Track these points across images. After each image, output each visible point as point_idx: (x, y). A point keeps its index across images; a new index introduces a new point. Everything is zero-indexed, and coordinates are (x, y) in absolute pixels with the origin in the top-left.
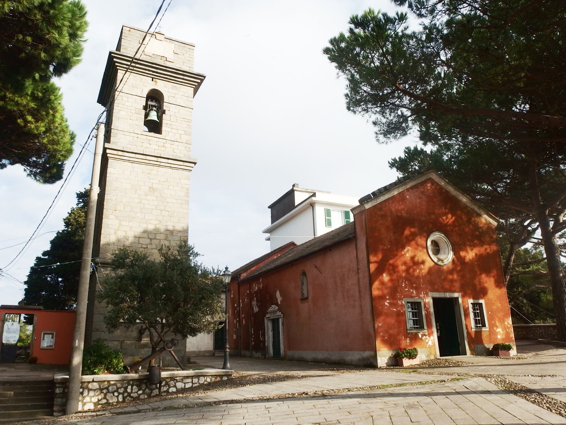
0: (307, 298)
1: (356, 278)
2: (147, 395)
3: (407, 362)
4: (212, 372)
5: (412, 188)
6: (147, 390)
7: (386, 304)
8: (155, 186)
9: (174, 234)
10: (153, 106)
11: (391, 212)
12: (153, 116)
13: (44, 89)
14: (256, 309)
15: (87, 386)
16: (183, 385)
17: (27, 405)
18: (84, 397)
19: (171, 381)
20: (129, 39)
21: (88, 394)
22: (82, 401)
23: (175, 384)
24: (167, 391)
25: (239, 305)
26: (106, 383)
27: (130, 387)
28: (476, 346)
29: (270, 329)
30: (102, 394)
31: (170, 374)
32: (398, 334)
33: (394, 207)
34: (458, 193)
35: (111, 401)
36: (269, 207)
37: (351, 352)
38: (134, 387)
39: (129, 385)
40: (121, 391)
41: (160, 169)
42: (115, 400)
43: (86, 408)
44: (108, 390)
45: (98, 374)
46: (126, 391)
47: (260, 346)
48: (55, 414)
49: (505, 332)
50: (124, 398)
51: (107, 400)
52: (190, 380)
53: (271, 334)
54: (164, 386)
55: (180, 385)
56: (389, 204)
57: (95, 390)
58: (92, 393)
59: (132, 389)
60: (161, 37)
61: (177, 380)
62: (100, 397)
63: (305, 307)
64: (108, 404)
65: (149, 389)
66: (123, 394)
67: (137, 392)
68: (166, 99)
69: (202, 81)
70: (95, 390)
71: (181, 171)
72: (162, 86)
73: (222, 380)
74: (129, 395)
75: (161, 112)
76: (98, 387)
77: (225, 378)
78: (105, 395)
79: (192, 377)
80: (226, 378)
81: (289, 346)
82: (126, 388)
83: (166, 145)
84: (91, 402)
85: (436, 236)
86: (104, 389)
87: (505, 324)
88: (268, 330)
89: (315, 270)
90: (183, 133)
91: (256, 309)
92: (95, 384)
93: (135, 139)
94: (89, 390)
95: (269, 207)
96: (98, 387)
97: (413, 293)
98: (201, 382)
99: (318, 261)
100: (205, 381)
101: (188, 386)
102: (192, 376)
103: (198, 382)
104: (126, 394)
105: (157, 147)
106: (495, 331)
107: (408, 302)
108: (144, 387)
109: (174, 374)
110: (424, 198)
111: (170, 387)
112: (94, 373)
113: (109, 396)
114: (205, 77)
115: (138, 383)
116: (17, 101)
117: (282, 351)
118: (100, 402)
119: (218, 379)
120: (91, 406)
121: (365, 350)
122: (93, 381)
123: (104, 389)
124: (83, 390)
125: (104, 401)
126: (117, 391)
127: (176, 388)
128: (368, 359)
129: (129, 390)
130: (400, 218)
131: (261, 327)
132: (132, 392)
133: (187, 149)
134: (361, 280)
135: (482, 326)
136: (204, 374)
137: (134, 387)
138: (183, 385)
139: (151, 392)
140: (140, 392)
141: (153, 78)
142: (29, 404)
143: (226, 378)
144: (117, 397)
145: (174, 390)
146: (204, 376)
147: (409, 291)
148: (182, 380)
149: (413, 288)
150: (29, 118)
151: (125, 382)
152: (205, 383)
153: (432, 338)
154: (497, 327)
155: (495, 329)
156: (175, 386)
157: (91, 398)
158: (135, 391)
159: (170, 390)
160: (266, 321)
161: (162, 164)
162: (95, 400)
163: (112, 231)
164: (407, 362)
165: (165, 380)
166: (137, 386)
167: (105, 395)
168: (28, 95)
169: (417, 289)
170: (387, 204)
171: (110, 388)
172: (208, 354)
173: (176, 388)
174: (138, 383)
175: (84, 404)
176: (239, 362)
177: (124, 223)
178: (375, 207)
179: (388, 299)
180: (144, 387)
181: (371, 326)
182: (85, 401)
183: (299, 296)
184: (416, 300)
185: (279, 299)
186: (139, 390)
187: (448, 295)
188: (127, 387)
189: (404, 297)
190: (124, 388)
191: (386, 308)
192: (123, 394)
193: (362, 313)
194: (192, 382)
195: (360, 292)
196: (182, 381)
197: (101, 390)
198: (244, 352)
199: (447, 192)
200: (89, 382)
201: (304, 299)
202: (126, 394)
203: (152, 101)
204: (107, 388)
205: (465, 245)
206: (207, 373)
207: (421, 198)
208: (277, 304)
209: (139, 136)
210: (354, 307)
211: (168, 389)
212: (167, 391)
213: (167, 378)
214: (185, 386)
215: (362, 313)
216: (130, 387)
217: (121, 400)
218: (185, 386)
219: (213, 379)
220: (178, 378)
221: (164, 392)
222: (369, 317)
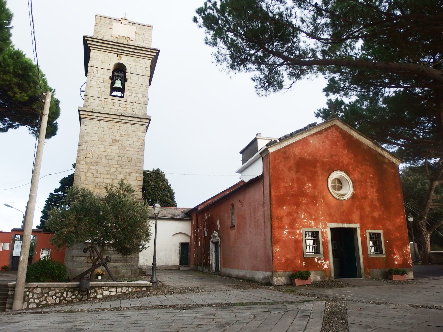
0: (234, 226)
1: (263, 210)
2: (79, 299)
3: (298, 282)
5: (316, 134)
6: (79, 296)
7: (285, 232)
8: (117, 138)
9: (131, 175)
10: (118, 76)
11: (295, 155)
12: (118, 84)
14: (206, 234)
16: (109, 293)
20: (100, 25)
23: (102, 292)
24: (95, 298)
25: (197, 231)
27: (65, 293)
28: (372, 270)
29: (214, 251)
32: (295, 259)
34: (362, 137)
36: (240, 153)
37: (258, 272)
38: (69, 293)
40: (59, 295)
41: (122, 125)
44: (48, 294)
46: (62, 295)
47: (207, 264)
49: (402, 258)
50: (60, 301)
51: (47, 302)
52: (114, 289)
53: (214, 254)
54: (93, 293)
55: (106, 293)
56: (293, 148)
59: (67, 294)
60: (126, 22)
61: (104, 289)
63: (233, 233)
66: (60, 297)
67: (71, 297)
68: (128, 70)
69: (158, 54)
71: (138, 126)
72: (125, 60)
74: (64, 299)
75: (124, 81)
78: (46, 297)
81: (224, 265)
82: (62, 293)
83: (127, 106)
84: (34, 302)
85: (336, 174)
87: (403, 252)
88: (212, 251)
89: (239, 203)
90: (141, 96)
91: (206, 234)
92: (39, 289)
93: (103, 102)
95: (240, 153)
97: (311, 223)
98: (123, 291)
99: (241, 197)
100: (127, 290)
101: (112, 294)
102: (117, 287)
104: (62, 298)
105: (119, 108)
106: (392, 257)
107: (306, 232)
108: (77, 293)
110: (327, 142)
111: (97, 294)
114: (159, 51)
117: (219, 269)
118: (42, 303)
121: (266, 271)
122: (37, 287)
124: (29, 294)
126: (55, 295)
127: (103, 295)
128: (265, 278)
129: (65, 295)
130: (302, 160)
131: (208, 249)
132: (66, 297)
133: (144, 108)
134: (265, 212)
135: (379, 253)
138: (109, 293)
139: (82, 297)
140: (74, 297)
141: (118, 54)
144: (55, 299)
145: (101, 296)
147: (308, 222)
149: (311, 219)
150: (17, 90)
151: (62, 288)
152: (127, 292)
153: (328, 262)
154: (395, 254)
155: (392, 255)
156: (102, 294)
157: (34, 300)
158: (69, 296)
161: (132, 122)
163: (83, 173)
164: (298, 282)
166: (71, 292)
168: (11, 73)
169: (315, 220)
170: (291, 148)
171: (50, 293)
172: (175, 268)
173: (103, 295)
174: (72, 290)
176: (184, 276)
177: (92, 167)
178: (278, 151)
179: (287, 229)
180: (77, 293)
181: (270, 251)
183: (230, 224)
184: (315, 229)
185: (219, 226)
187: (346, 226)
189: (303, 227)
191: (284, 236)
193: (265, 240)
194: (116, 291)
195: (265, 222)
198: (200, 268)
199: (351, 137)
200: (34, 288)
201: (233, 227)
202: (62, 298)
203: (118, 72)
207: (325, 142)
208: (217, 231)
209: (106, 100)
210: (261, 235)
211: (96, 296)
212: (95, 298)
215: (265, 240)
216: (65, 293)
220: (105, 288)
221: (93, 297)
222: (269, 242)
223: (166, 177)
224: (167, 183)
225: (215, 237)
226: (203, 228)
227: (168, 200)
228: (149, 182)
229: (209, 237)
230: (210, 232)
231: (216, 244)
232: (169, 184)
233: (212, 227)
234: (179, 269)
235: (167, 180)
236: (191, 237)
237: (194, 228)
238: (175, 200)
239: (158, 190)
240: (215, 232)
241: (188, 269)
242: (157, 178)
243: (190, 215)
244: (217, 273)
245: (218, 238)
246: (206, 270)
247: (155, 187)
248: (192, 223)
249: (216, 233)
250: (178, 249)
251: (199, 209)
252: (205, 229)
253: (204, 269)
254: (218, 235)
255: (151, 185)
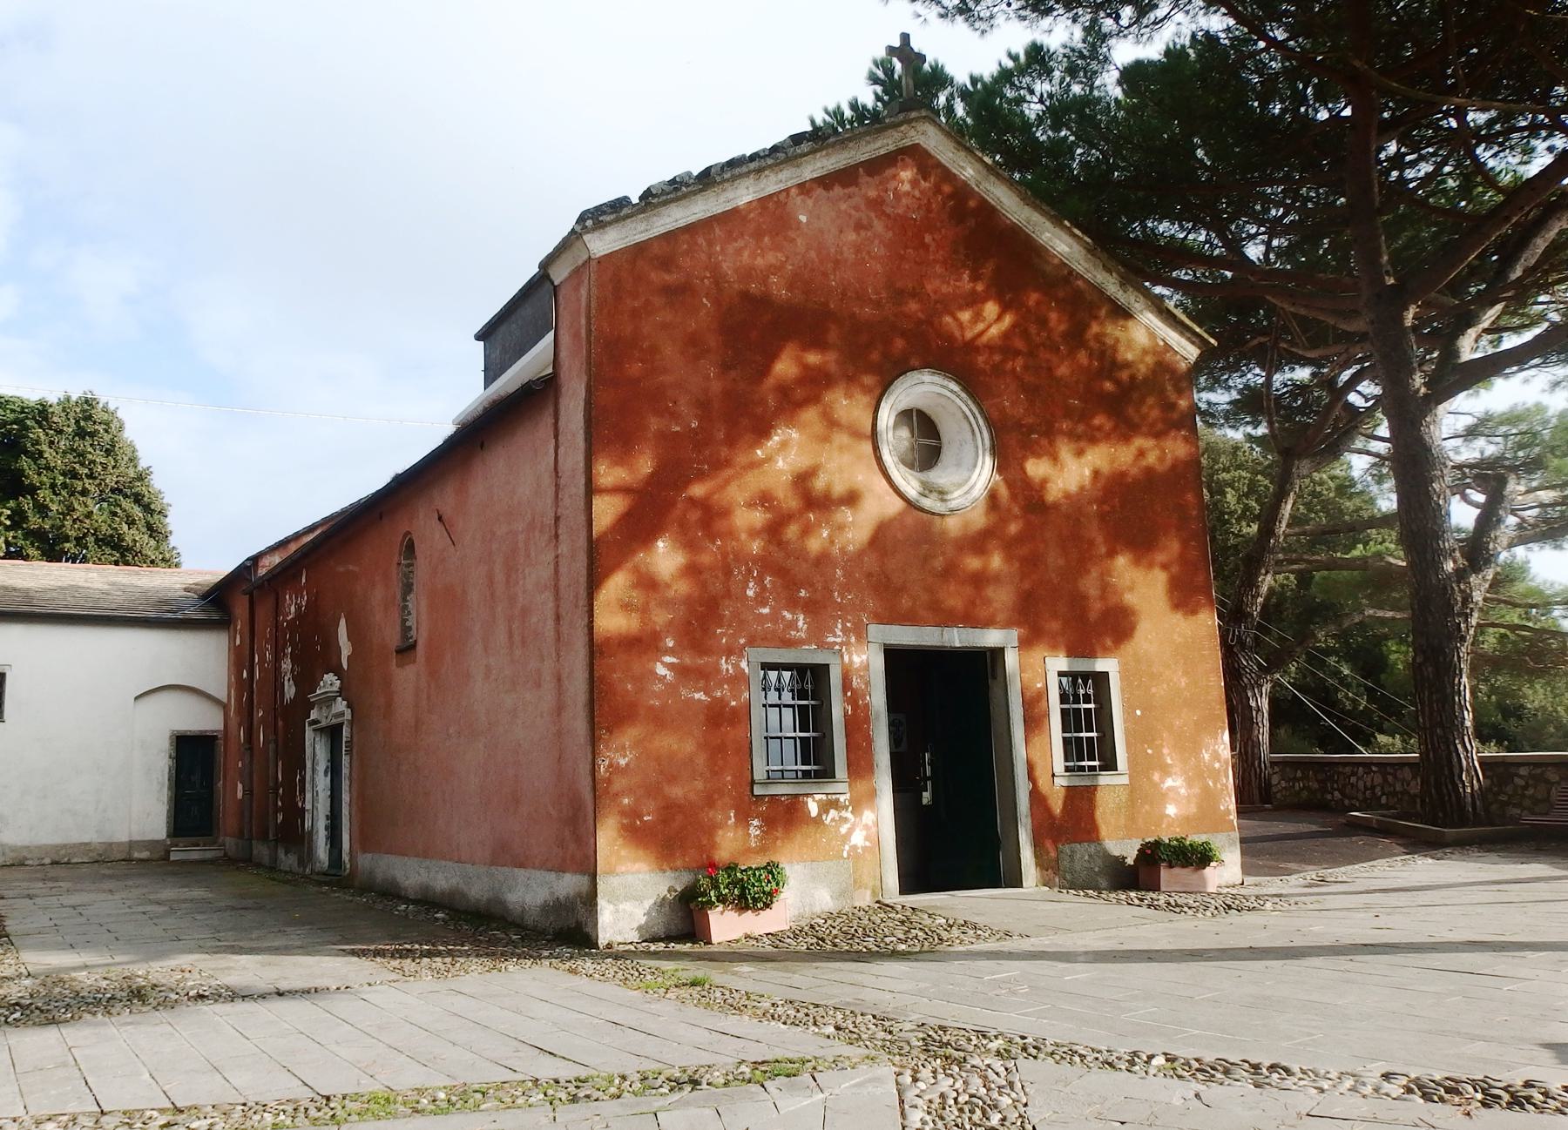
0: (413, 647)
1: (550, 557)
3: (725, 925)
5: (826, 181)
7: (661, 670)
11: (718, 278)
14: (290, 691)
28: (1067, 848)
32: (709, 801)
33: (738, 258)
34: (1036, 217)
36: (478, 337)
37: (521, 873)
47: (293, 834)
49: (1197, 790)
53: (323, 783)
56: (710, 244)
63: (407, 679)
81: (366, 841)
85: (923, 388)
87: (1199, 759)
89: (438, 532)
91: (290, 691)
95: (478, 337)
97: (792, 625)
99: (445, 497)
106: (1156, 786)
107: (766, 667)
110: (879, 226)
117: (345, 857)
121: (561, 869)
128: (558, 907)
130: (756, 303)
131: (295, 760)
134: (563, 570)
135: (1102, 768)
147: (775, 617)
149: (793, 604)
153: (868, 816)
154: (1166, 771)
155: (1156, 777)
160: (309, 733)
164: (725, 925)
169: (811, 608)
170: (701, 240)
172: (145, 855)
176: (168, 893)
178: (638, 251)
179: (671, 652)
181: (584, 768)
183: (393, 639)
184: (809, 655)
185: (346, 649)
187: (957, 638)
189: (752, 642)
191: (658, 687)
193: (559, 709)
195: (558, 618)
198: (261, 851)
199: (987, 211)
201: (407, 649)
205: (1050, 433)
207: (868, 227)
208: (338, 671)
210: (538, 685)
215: (559, 709)
222: (578, 724)
223: (129, 434)
224: (133, 460)
225: (329, 700)
226: (277, 659)
227: (134, 535)
228: (41, 453)
229: (303, 705)
230: (307, 682)
231: (333, 733)
232: (142, 464)
233: (314, 655)
234: (166, 858)
235: (131, 445)
236: (225, 707)
237: (241, 660)
238: (173, 541)
239: (84, 492)
240: (330, 678)
241: (209, 855)
242: (81, 433)
243: (219, 604)
244: (337, 877)
245: (340, 705)
246: (288, 861)
247: (75, 475)
248: (232, 639)
249: (330, 682)
250: (161, 763)
251: (262, 572)
252: (287, 665)
253: (281, 854)
254: (341, 692)
255: (48, 468)
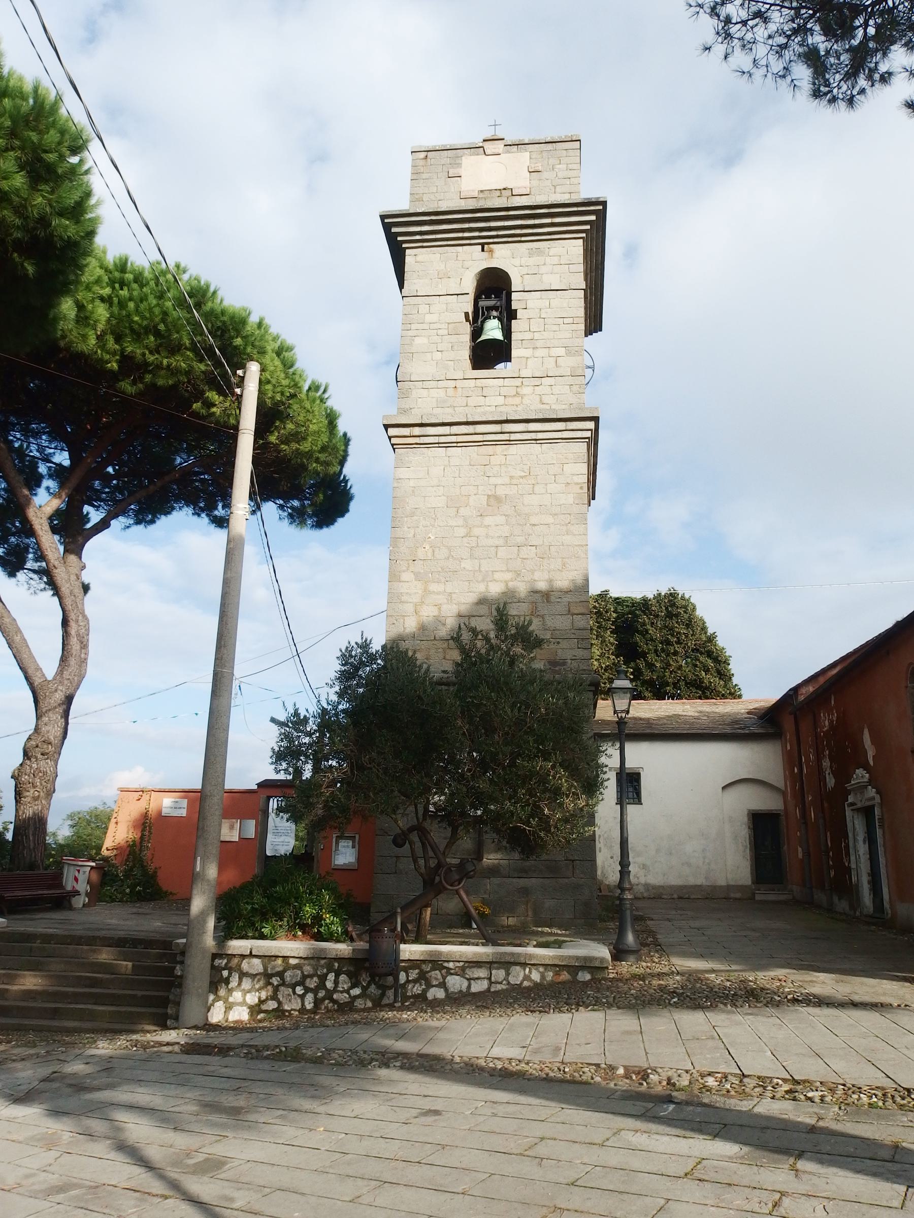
2: (373, 1001)
4: (544, 957)
6: (373, 989)
8: (501, 491)
9: (553, 599)
10: (489, 309)
12: (493, 330)
13: (219, 328)
14: (831, 782)
15: (239, 965)
16: (466, 983)
17: (134, 996)
18: (230, 991)
19: (433, 969)
20: (424, 176)
21: (239, 984)
22: (226, 1001)
23: (444, 978)
24: (422, 997)
25: (801, 770)
26: (279, 961)
27: (331, 977)
29: (861, 837)
30: (270, 987)
31: (431, 953)
35: (286, 1007)
38: (343, 977)
39: (329, 971)
40: (312, 983)
41: (513, 449)
42: (296, 1004)
43: (234, 1016)
44: (282, 978)
45: (273, 938)
46: (322, 985)
47: (843, 884)
48: (168, 1022)
50: (317, 1002)
51: (280, 1003)
52: (482, 973)
53: (863, 849)
54: (415, 981)
55: (456, 983)
57: (253, 976)
58: (247, 984)
59: (336, 982)
60: (499, 146)
61: (448, 969)
62: (264, 995)
64: (280, 1013)
65: (379, 987)
66: (315, 991)
67: (348, 992)
68: (516, 285)
69: (602, 215)
70: (253, 976)
71: (562, 446)
72: (505, 257)
73: (574, 982)
74: (329, 995)
75: (508, 316)
76: (260, 969)
77: (585, 976)
78: (276, 989)
79: (490, 965)
80: (588, 977)
82: (323, 978)
83: (525, 390)
84: (244, 1003)
86: (273, 976)
88: (855, 840)
90: (562, 351)
91: (831, 782)
92: (256, 961)
93: (451, 392)
94: (243, 975)
96: (260, 969)
98: (512, 980)
100: (527, 978)
101: (476, 987)
102: (491, 963)
103: (506, 979)
104: (321, 994)
105: (501, 400)
108: (364, 978)
109: (440, 953)
111: (429, 986)
112: (262, 937)
113: (284, 991)
114: (604, 204)
115: (352, 969)
116: (169, 366)
117: (887, 905)
118: (264, 1007)
119: (565, 976)
120: (240, 1014)
122: (251, 955)
123: (273, 976)
124: (230, 974)
125: (272, 1005)
126: (301, 983)
127: (446, 990)
129: (329, 985)
131: (840, 832)
132: (335, 990)
133: (575, 388)
136: (522, 960)
137: (343, 977)
138: (466, 983)
139: (383, 995)
140: (356, 991)
141: (483, 245)
142: (140, 993)
143: (588, 977)
144: (302, 997)
145: (440, 994)
146: (524, 965)
148: (463, 969)
150: (213, 396)
151: (323, 962)
152: (526, 984)
156: (443, 985)
157: (244, 995)
158: (343, 988)
159: (430, 995)
160: (848, 813)
162: (252, 999)
163: (409, 608)
165: (418, 967)
166: (350, 975)
167: (276, 989)
168: (186, 348)
171: (288, 974)
172: (738, 895)
173: (446, 990)
174: (352, 969)
175: (229, 1008)
177: (433, 587)
180: (364, 978)
182: (231, 999)
185: (871, 753)
186: (353, 986)
188: (327, 975)
190: (319, 976)
192: (315, 991)
194: (490, 979)
196: (461, 972)
197: (267, 976)
198: (821, 897)
200: (243, 957)
202: (321, 994)
203: (488, 297)
204: (281, 974)
206: (531, 956)
208: (866, 767)
209: (459, 384)
211: (425, 992)
212: (422, 997)
213: (423, 961)
214: (469, 987)
216: (331, 977)
217: (309, 1006)
218: (469, 987)
219: (550, 975)
220: (451, 965)
221: (416, 996)
223: (699, 613)
224: (704, 629)
225: (862, 788)
226: (819, 759)
227: (708, 678)
228: (647, 631)
229: (841, 792)
230: (843, 775)
231: (867, 812)
232: (710, 631)
233: (847, 757)
234: (752, 897)
235: (702, 620)
236: (784, 793)
237: (792, 761)
238: (735, 680)
239: (676, 653)
240: (860, 772)
241: (782, 898)
242: (670, 615)
243: (771, 723)
244: (880, 918)
245: (871, 792)
246: (842, 905)
247: (668, 643)
248: (784, 747)
249: (861, 775)
250: (744, 833)
251: (801, 698)
252: (826, 763)
253: (836, 899)
254: (870, 782)
255: (652, 640)
